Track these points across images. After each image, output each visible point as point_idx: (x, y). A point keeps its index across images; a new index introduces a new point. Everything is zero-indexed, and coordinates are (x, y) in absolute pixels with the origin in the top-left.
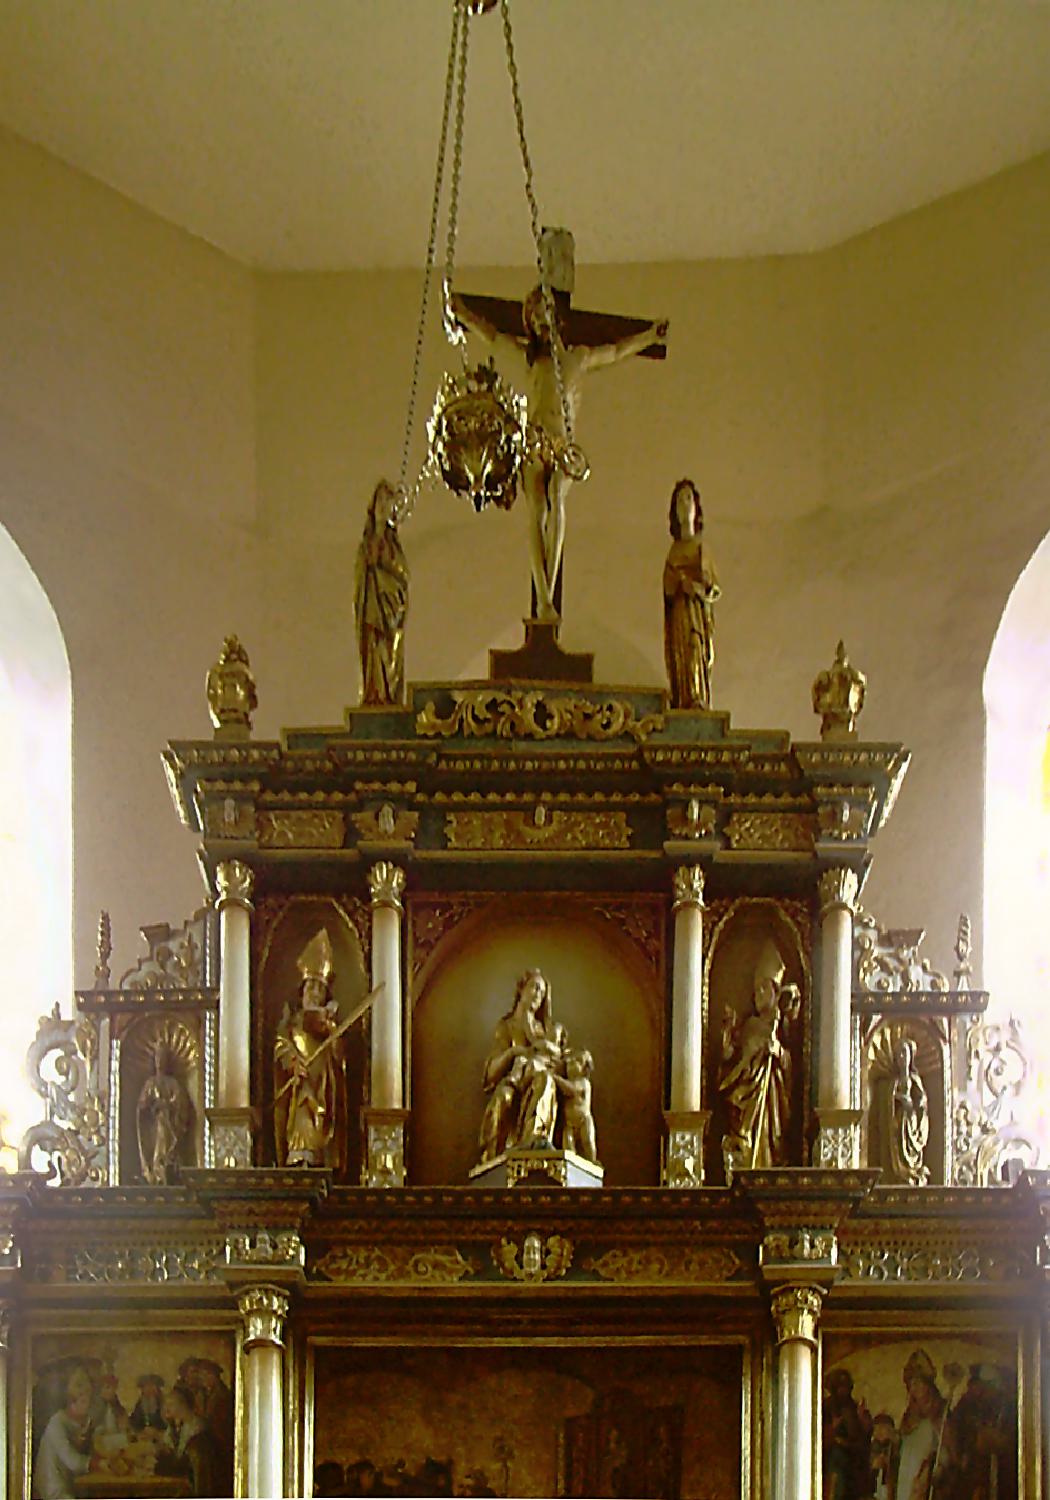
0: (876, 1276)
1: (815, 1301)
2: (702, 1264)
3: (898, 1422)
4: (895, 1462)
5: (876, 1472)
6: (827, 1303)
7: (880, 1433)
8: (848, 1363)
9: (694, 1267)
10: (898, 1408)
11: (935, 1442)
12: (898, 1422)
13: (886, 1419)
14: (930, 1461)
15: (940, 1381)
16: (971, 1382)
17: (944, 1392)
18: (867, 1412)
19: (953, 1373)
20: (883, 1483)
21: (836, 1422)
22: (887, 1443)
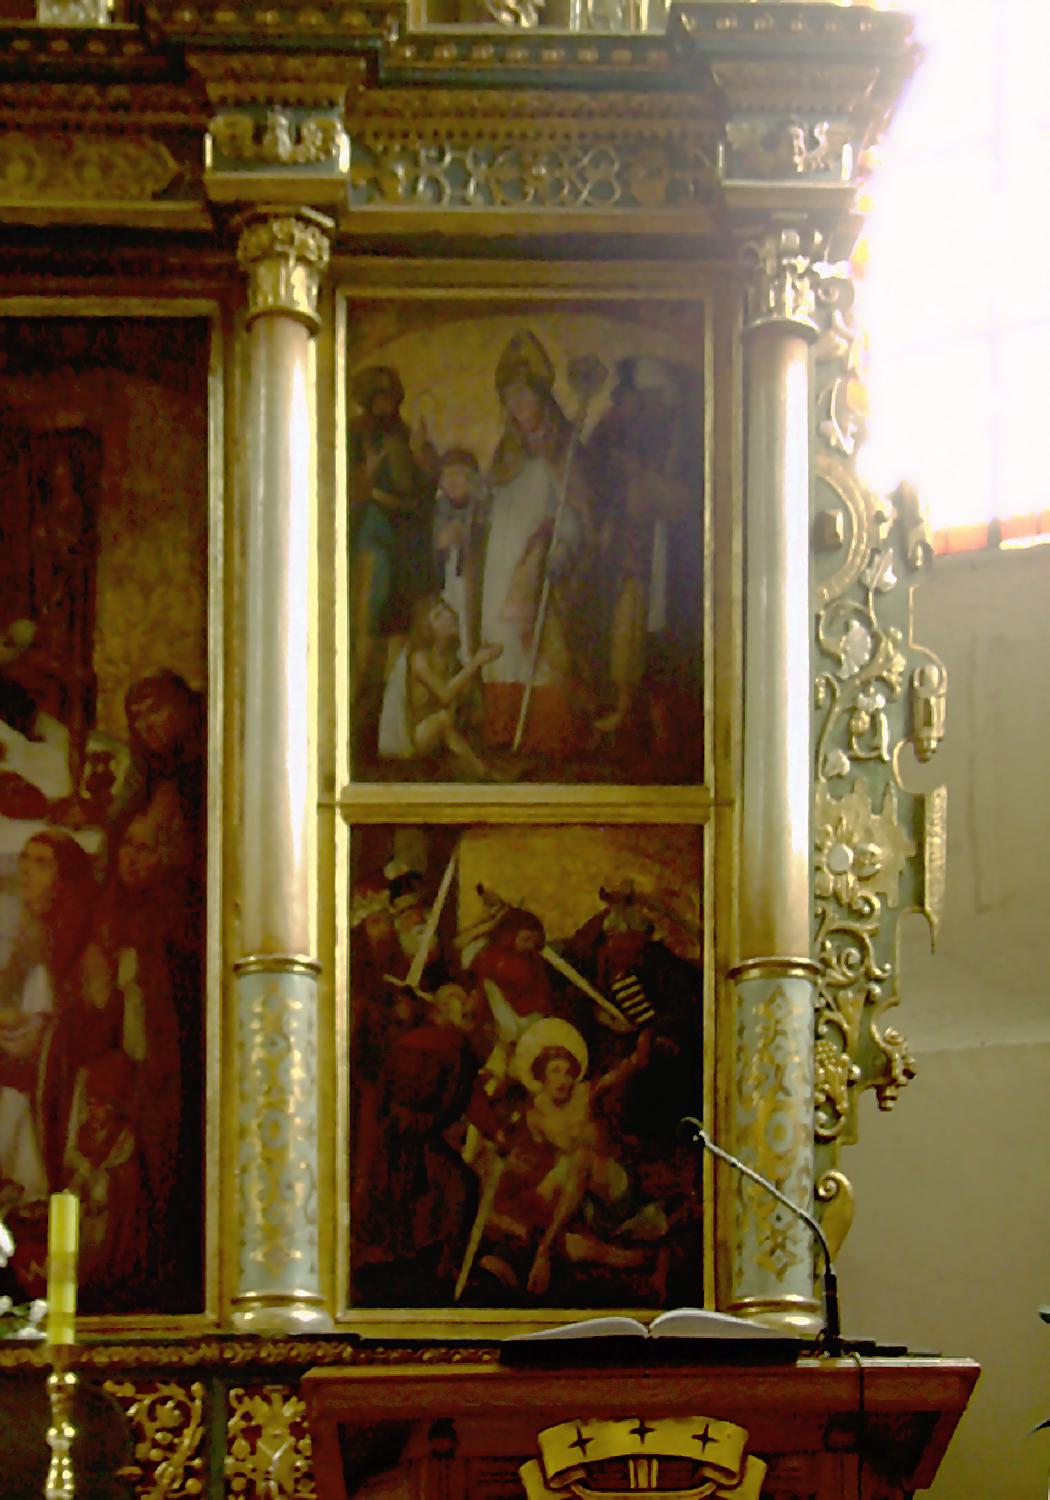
0: (429, 194)
1: (315, 244)
2: (106, 167)
3: (485, 463)
4: (477, 541)
5: (443, 556)
6: (341, 244)
7: (453, 482)
8: (394, 356)
9: (92, 172)
10: (485, 437)
11: (552, 500)
12: (485, 463)
13: (465, 457)
15: (561, 387)
16: (617, 395)
17: (570, 410)
18: (428, 446)
19: (585, 375)
20: (459, 573)
21: (372, 462)
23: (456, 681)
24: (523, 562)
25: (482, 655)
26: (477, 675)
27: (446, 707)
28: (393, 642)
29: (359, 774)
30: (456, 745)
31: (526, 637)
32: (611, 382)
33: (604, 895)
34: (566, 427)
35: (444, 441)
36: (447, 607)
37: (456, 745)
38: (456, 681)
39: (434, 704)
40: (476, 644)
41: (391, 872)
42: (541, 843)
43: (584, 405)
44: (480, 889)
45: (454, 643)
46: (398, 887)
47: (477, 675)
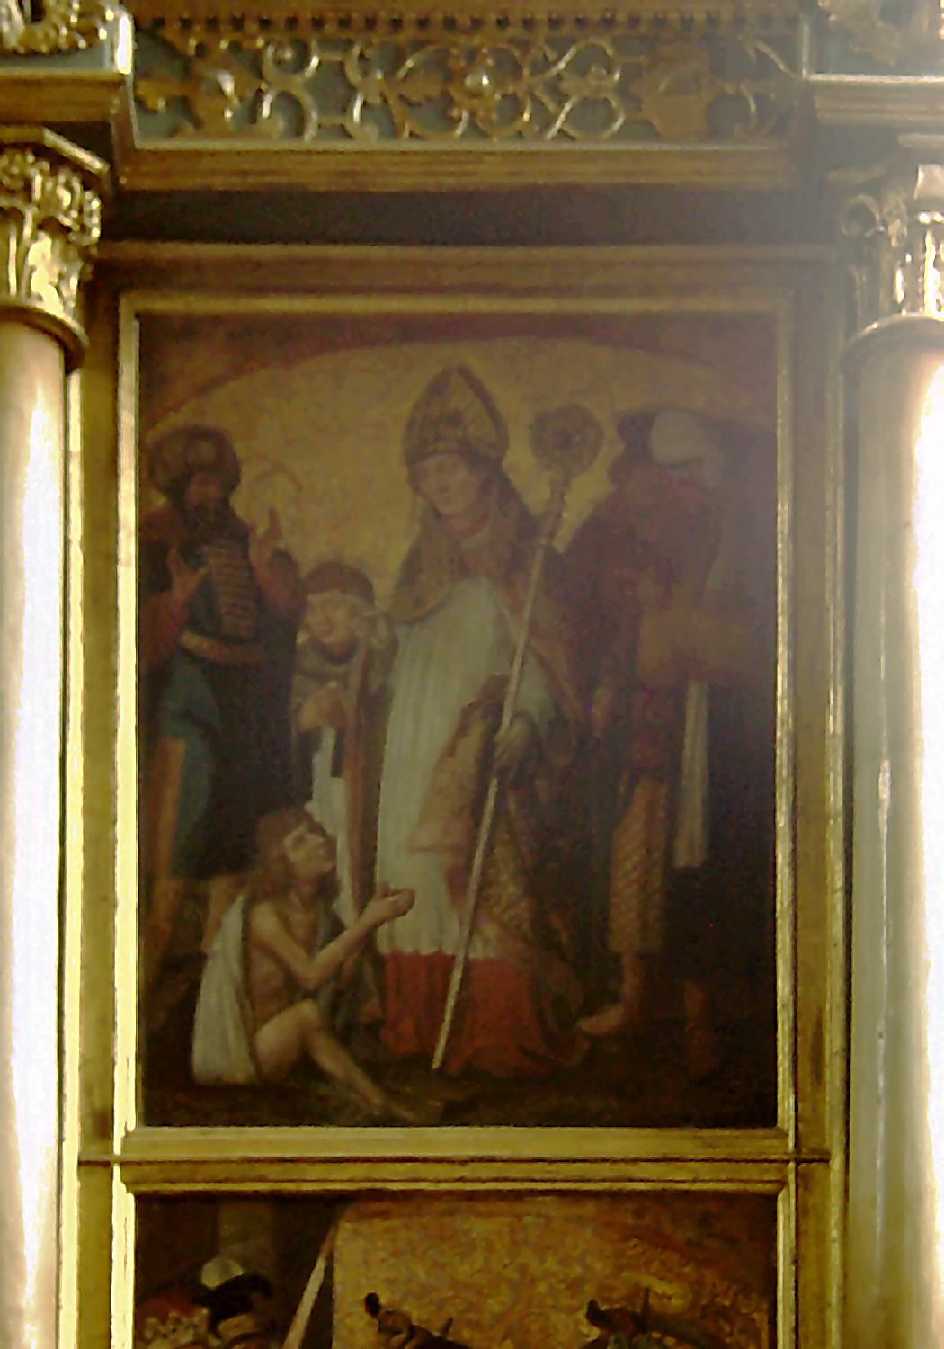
5: (309, 742)
8: (219, 411)
11: (504, 646)
12: (383, 587)
14: (490, 703)
15: (520, 459)
16: (618, 472)
17: (536, 495)
18: (284, 559)
20: (336, 771)
21: (183, 586)
22: (343, 655)
23: (332, 951)
24: (451, 751)
25: (376, 908)
26: (367, 941)
27: (311, 995)
28: (217, 888)
29: (154, 1111)
30: (330, 1058)
31: (456, 881)
32: (612, 449)
33: (595, 1316)
34: (528, 526)
35: (310, 552)
36: (317, 829)
37: (330, 1058)
38: (332, 951)
39: (292, 990)
40: (366, 889)
41: (211, 1277)
42: (478, 1227)
43: (561, 488)
44: (372, 1303)
45: (326, 887)
46: (225, 1302)
47: (367, 941)
